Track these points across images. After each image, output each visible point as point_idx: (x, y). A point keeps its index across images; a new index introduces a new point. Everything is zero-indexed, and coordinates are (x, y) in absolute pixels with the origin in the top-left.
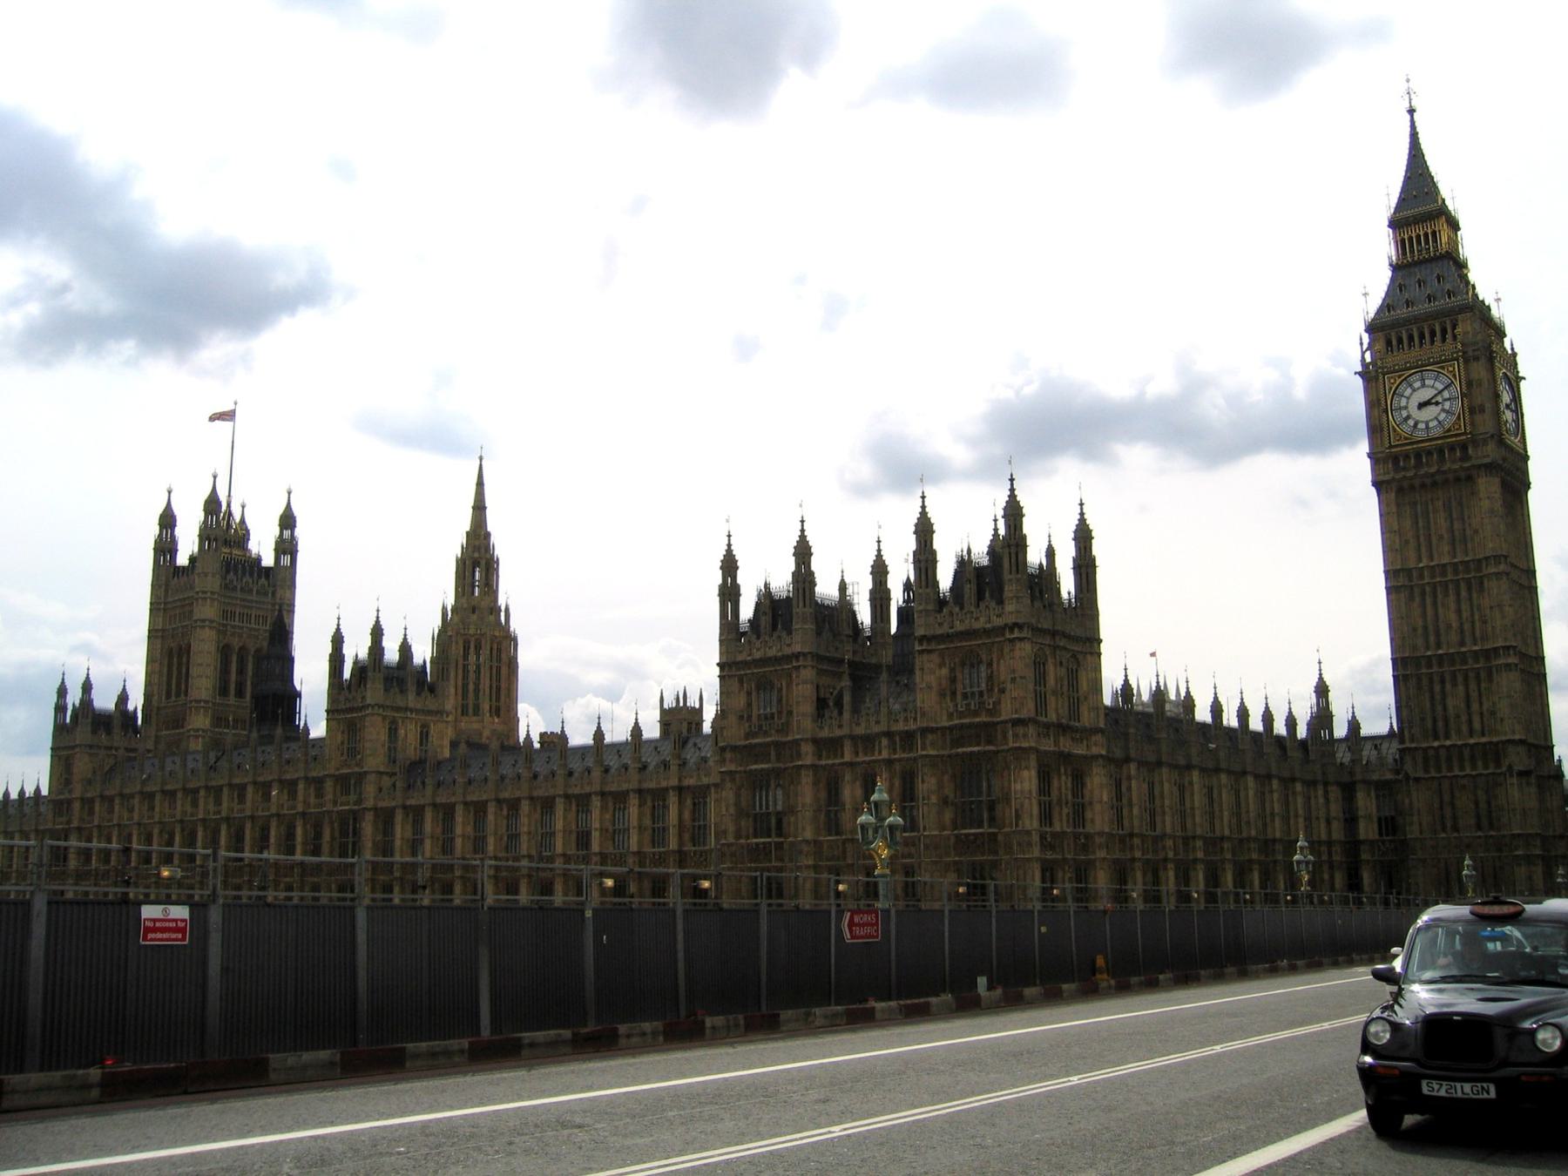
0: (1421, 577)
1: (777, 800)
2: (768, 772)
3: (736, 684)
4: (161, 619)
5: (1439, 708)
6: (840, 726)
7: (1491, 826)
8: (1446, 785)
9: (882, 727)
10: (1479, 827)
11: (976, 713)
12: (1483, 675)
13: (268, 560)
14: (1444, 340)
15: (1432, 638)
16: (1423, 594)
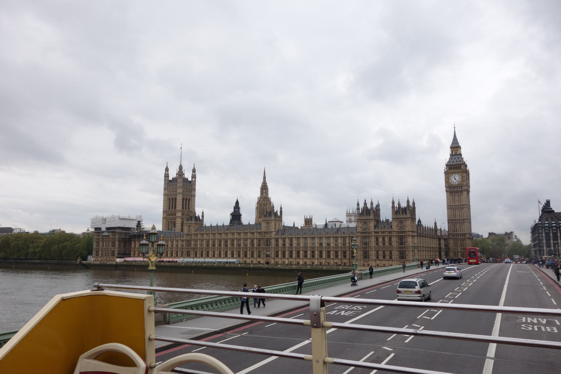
0: (453, 206)
1: (367, 240)
2: (366, 236)
3: (360, 223)
4: (167, 192)
5: (455, 228)
6: (378, 230)
7: (463, 246)
8: (456, 240)
9: (386, 230)
10: (461, 246)
11: (402, 229)
12: (463, 223)
13: (190, 179)
14: (459, 169)
15: (455, 217)
16: (453, 209)
